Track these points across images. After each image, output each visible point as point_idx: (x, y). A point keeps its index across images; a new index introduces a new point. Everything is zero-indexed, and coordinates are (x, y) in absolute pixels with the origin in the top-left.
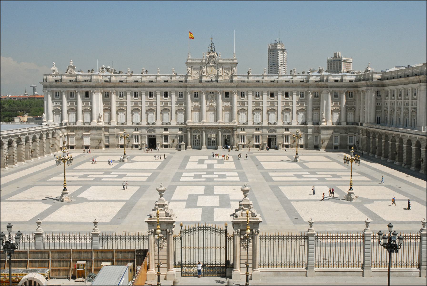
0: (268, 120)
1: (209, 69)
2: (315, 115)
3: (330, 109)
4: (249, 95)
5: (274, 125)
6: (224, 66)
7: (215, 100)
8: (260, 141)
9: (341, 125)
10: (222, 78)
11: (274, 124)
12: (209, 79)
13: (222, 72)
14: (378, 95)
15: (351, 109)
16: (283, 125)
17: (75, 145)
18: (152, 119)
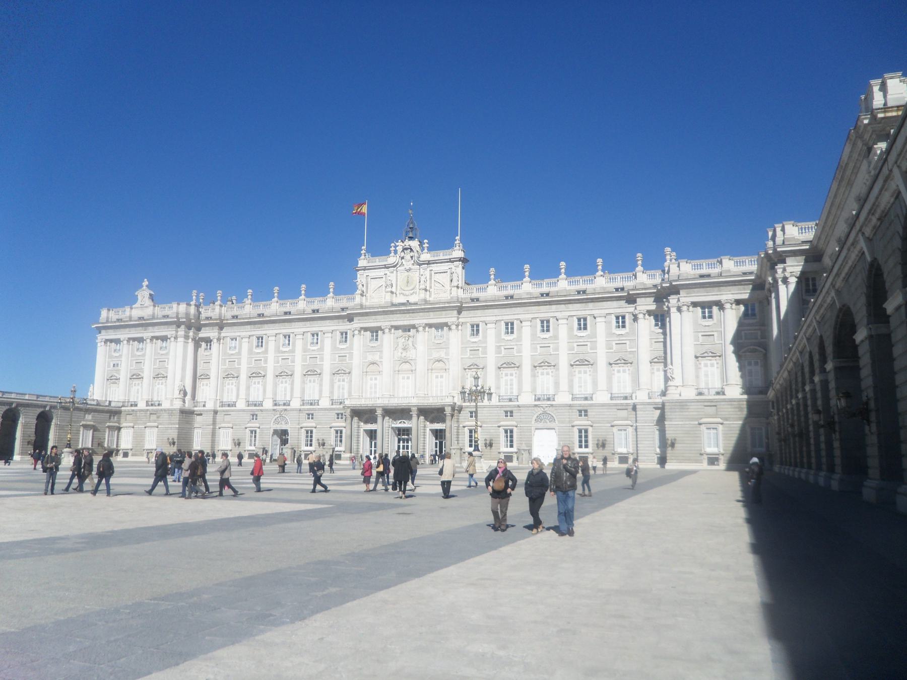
0: (534, 390)
1: (402, 275)
2: (656, 373)
3: (690, 351)
4: (489, 331)
5: (549, 403)
6: (435, 268)
7: (413, 346)
8: (515, 444)
9: (724, 394)
10: (430, 296)
11: (549, 399)
12: (402, 300)
13: (431, 283)
14: (808, 291)
15: (754, 351)
16: (572, 403)
17: (130, 447)
18: (285, 394)
